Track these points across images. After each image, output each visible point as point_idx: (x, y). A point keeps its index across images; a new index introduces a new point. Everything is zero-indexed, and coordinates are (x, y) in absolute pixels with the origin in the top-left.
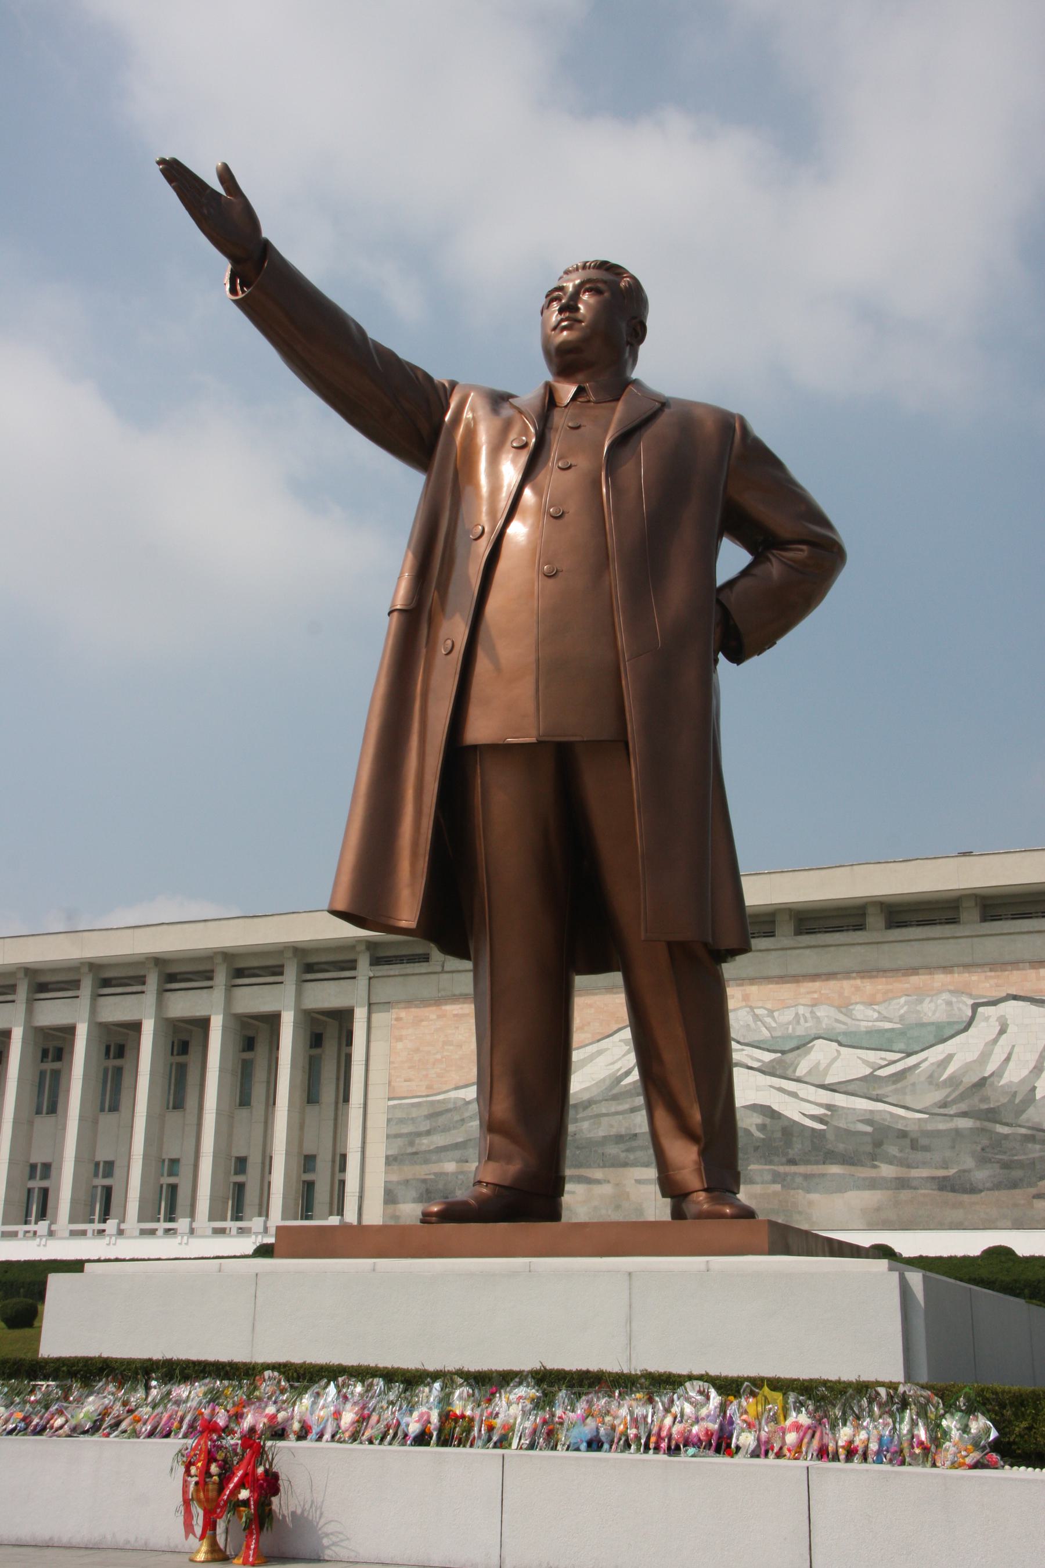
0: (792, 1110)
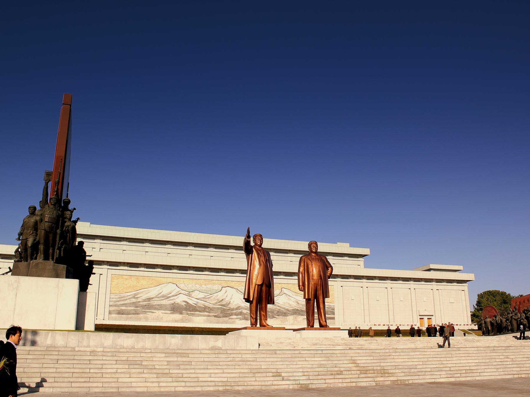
0: (191, 302)
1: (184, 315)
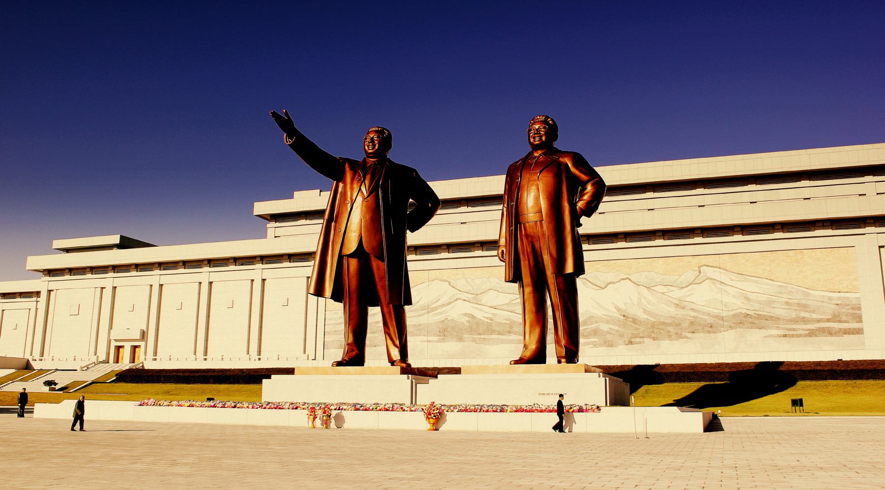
0: (479, 315)
1: (466, 343)
